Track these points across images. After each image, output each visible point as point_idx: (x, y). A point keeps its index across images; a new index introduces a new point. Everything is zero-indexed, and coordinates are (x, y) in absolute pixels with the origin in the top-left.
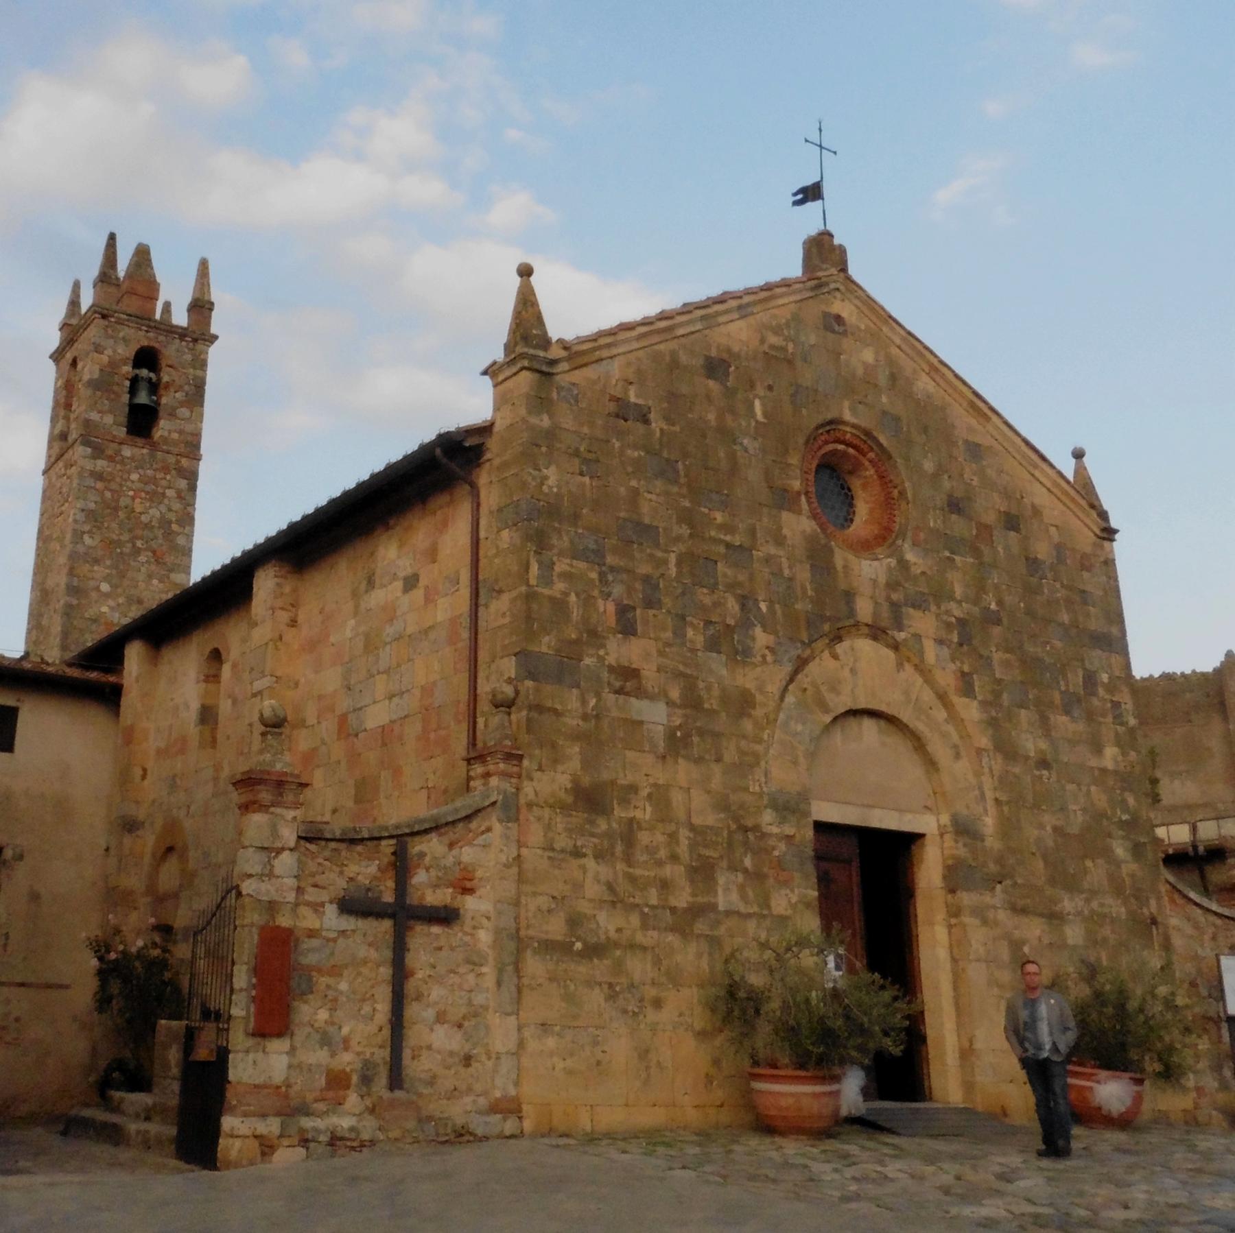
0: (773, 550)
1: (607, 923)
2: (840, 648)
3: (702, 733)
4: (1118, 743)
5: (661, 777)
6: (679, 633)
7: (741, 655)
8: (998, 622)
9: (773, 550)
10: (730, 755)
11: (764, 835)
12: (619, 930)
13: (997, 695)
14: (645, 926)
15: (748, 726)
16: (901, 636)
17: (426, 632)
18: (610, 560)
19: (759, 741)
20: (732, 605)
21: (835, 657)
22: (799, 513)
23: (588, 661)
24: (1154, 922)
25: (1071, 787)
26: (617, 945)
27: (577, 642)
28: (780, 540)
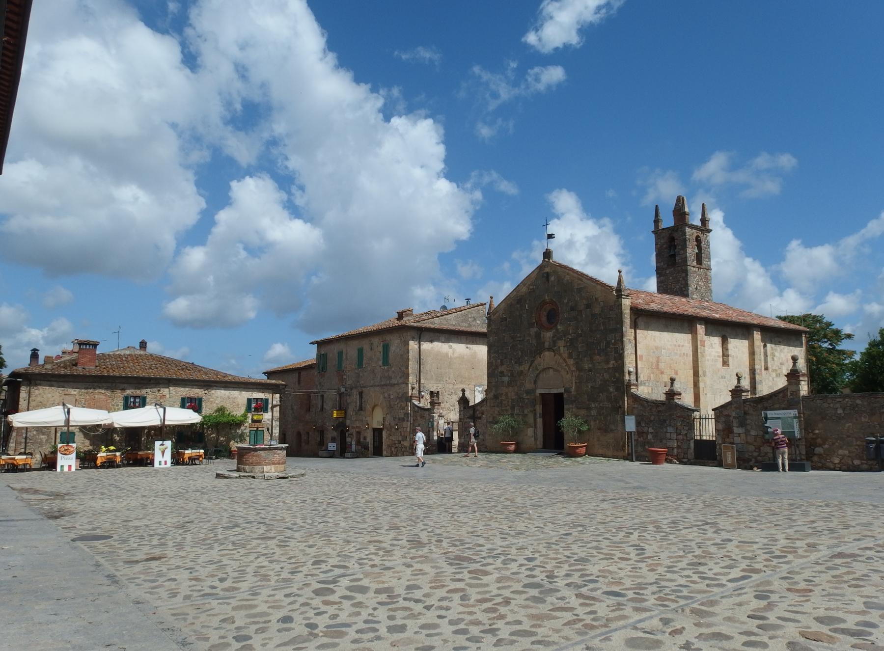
4: (615, 359)
7: (520, 364)
10: (518, 384)
28: (529, 335)
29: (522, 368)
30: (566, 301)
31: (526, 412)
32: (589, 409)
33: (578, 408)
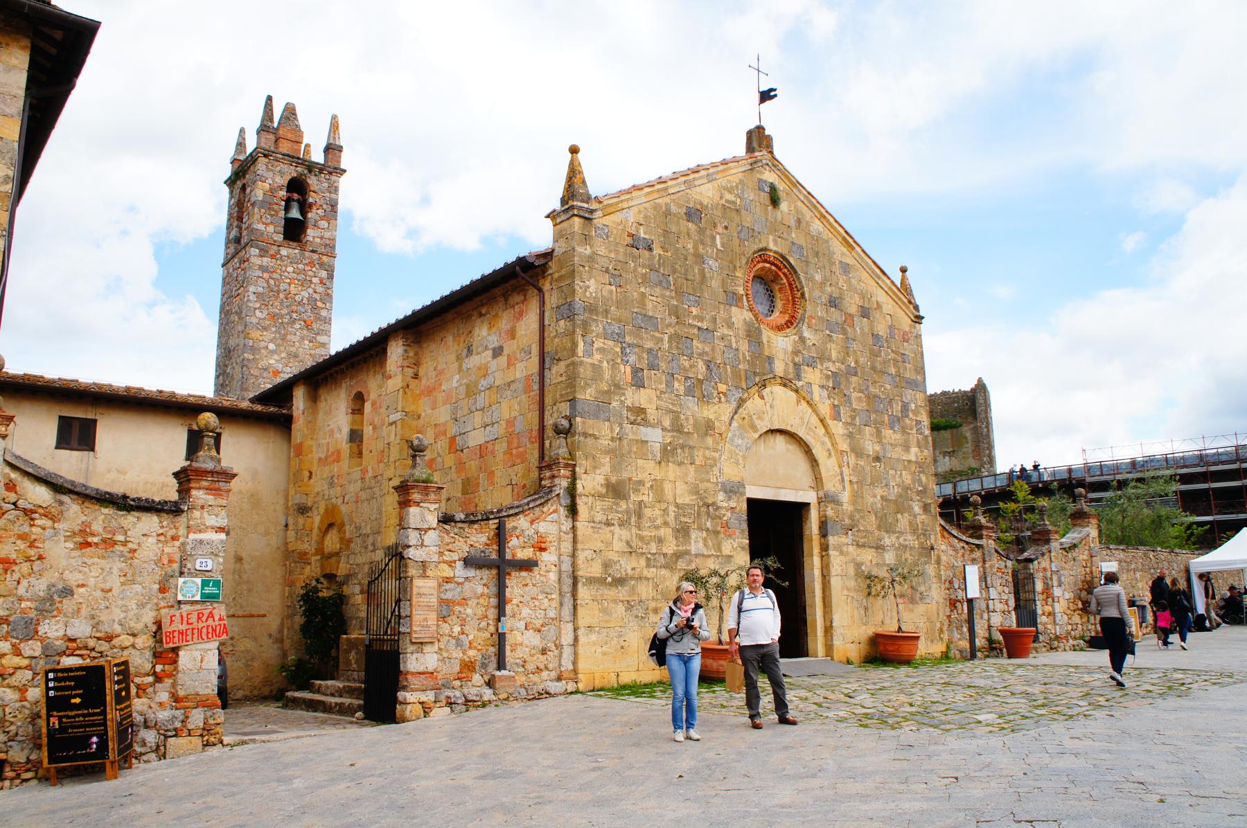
0: (725, 331)
1: (626, 566)
2: (766, 392)
3: (682, 447)
5: (658, 474)
6: (669, 384)
7: (705, 399)
8: (855, 374)
9: (725, 331)
11: (718, 508)
12: (633, 569)
13: (853, 418)
14: (648, 566)
15: (709, 440)
16: (799, 384)
17: (509, 384)
18: (627, 339)
19: (716, 450)
20: (701, 367)
21: (762, 398)
22: (742, 307)
23: (614, 404)
24: (932, 548)
25: (892, 472)
26: (632, 578)
27: (608, 392)
28: (730, 325)
29: (709, 412)
30: (818, 277)
31: (727, 548)
32: (879, 548)
33: (858, 545)
